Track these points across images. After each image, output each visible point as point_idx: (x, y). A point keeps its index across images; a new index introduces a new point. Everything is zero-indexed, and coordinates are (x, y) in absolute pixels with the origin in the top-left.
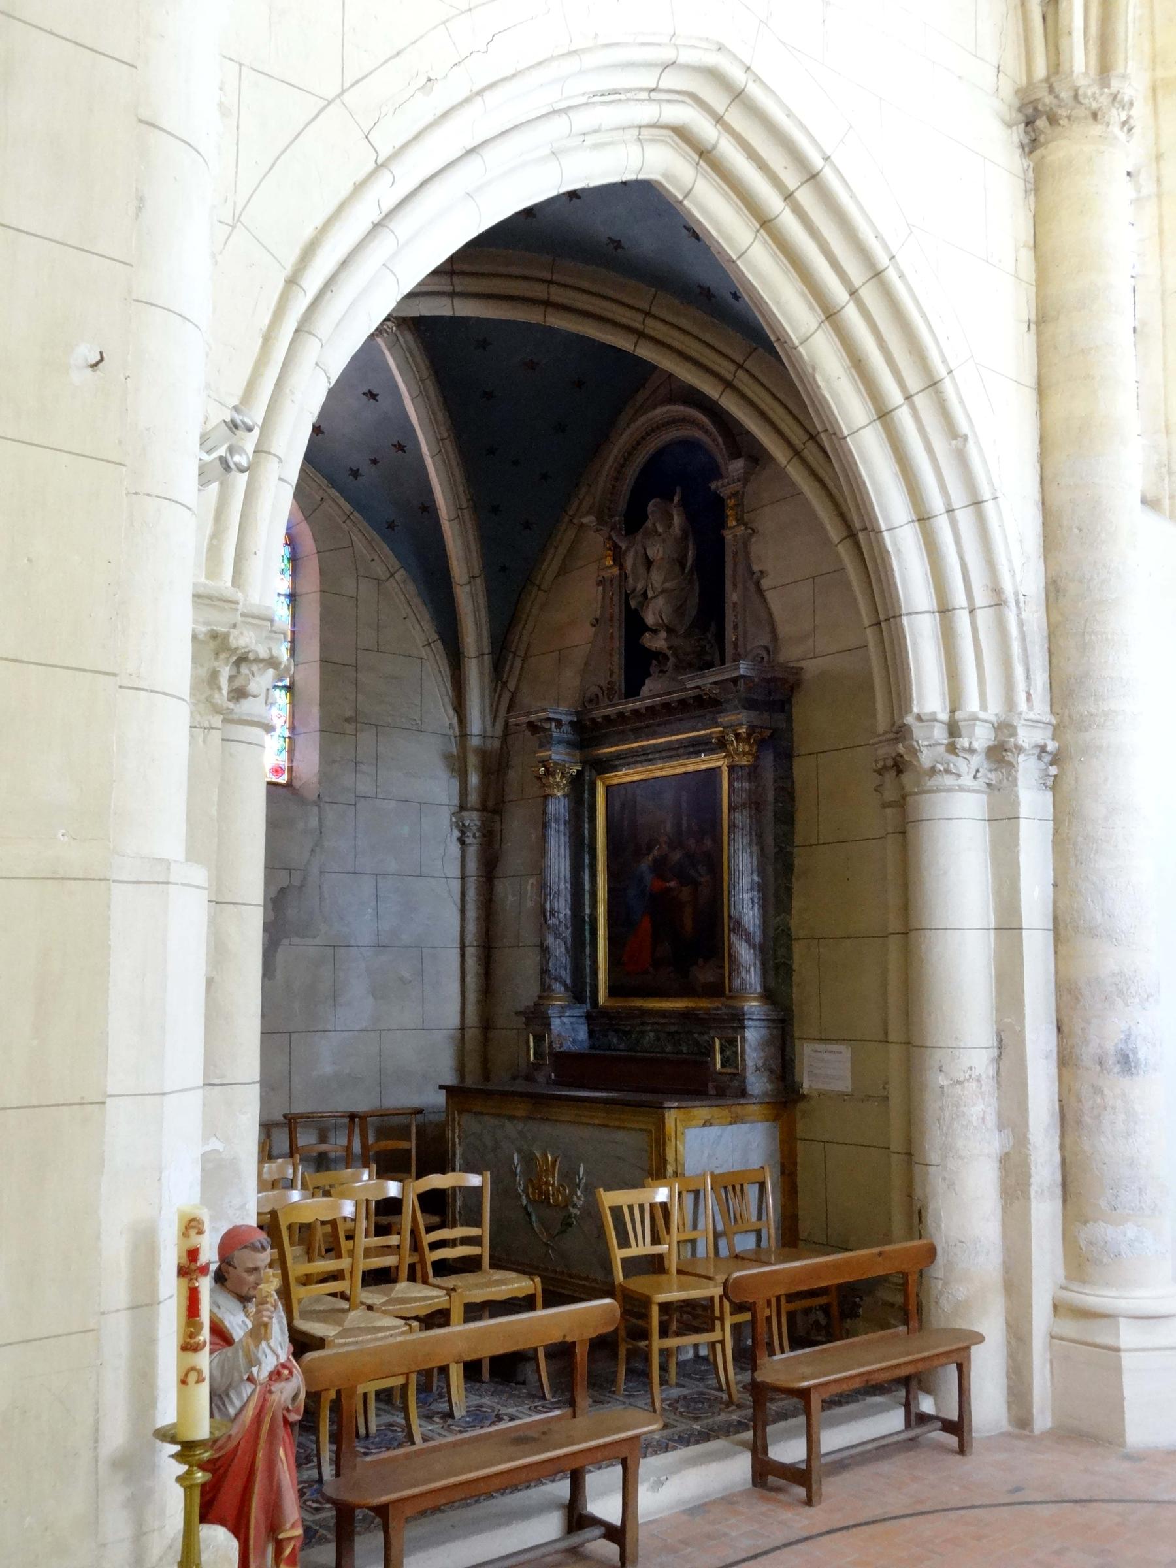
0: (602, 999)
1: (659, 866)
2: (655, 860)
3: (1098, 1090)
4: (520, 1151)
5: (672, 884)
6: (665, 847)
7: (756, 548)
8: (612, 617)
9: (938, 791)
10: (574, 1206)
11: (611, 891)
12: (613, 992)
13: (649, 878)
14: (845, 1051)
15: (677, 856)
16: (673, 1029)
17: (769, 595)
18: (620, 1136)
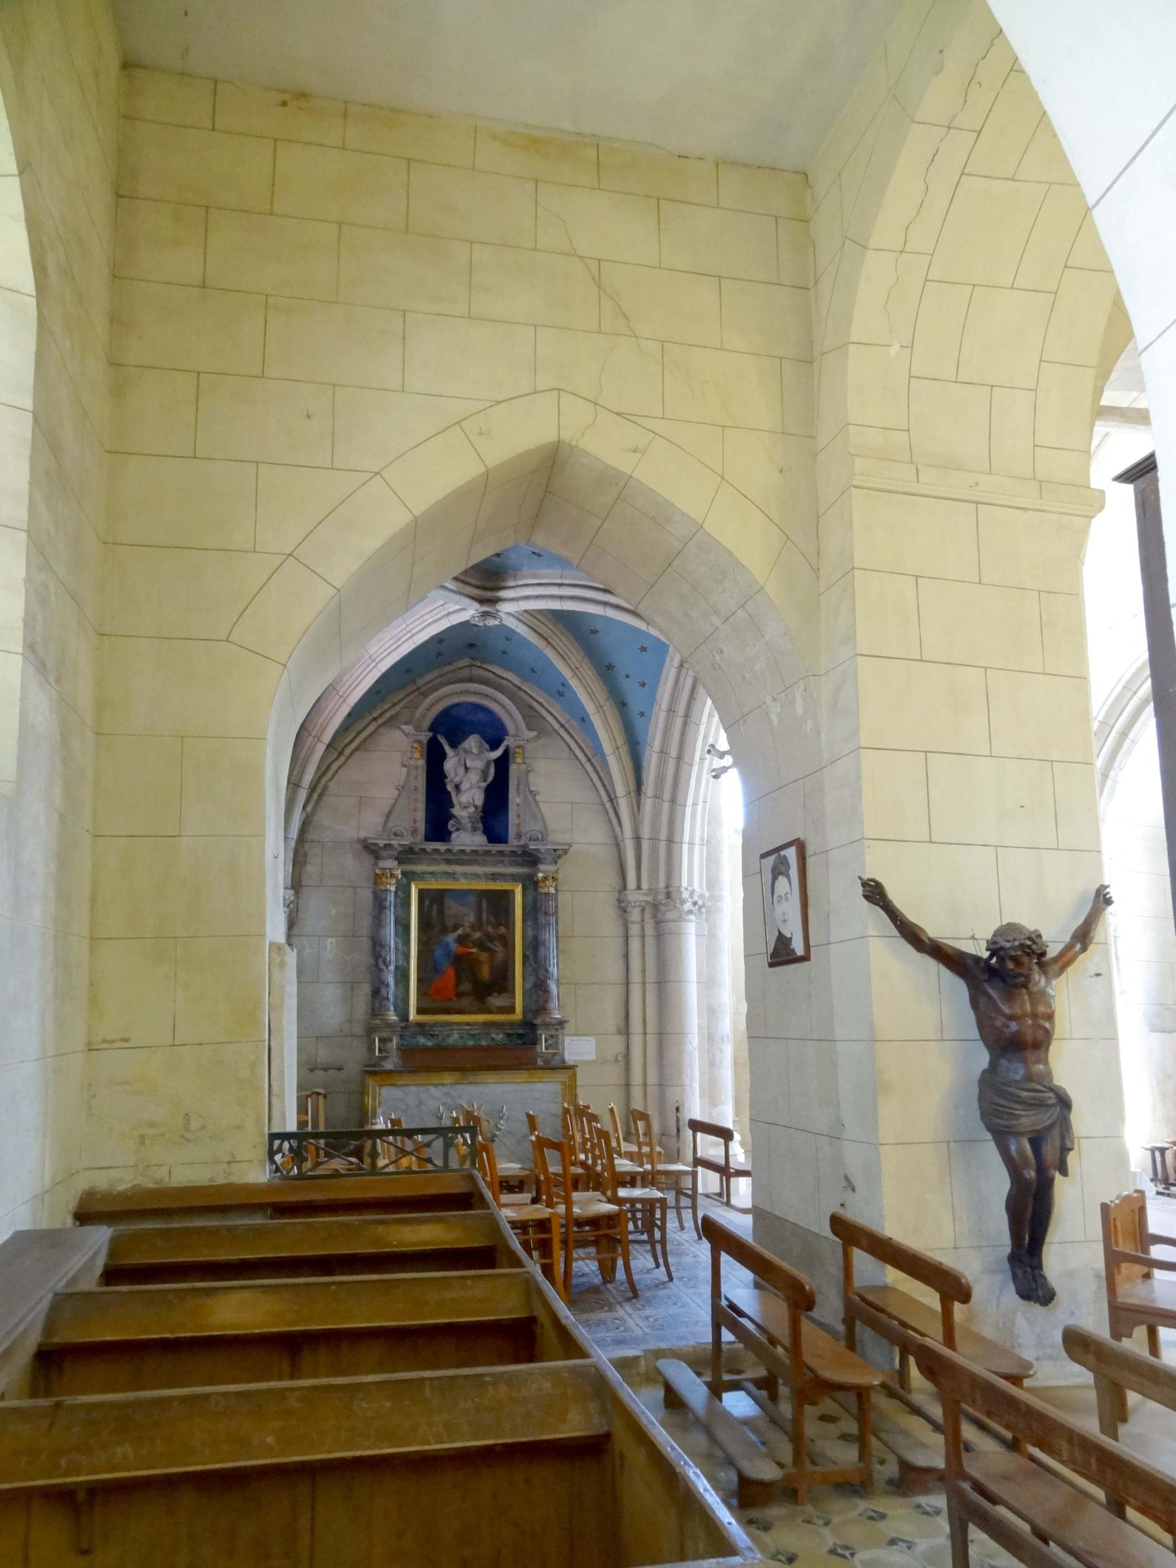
0: (412, 1015)
1: (462, 940)
2: (459, 936)
3: (721, 1051)
4: (444, 1104)
5: (474, 950)
6: (468, 930)
7: (532, 778)
8: (416, 788)
9: (669, 921)
10: (500, 1130)
11: (420, 952)
12: (420, 1011)
13: (454, 947)
14: (592, 1040)
15: (477, 935)
16: (475, 1032)
17: (541, 805)
18: (539, 1086)
